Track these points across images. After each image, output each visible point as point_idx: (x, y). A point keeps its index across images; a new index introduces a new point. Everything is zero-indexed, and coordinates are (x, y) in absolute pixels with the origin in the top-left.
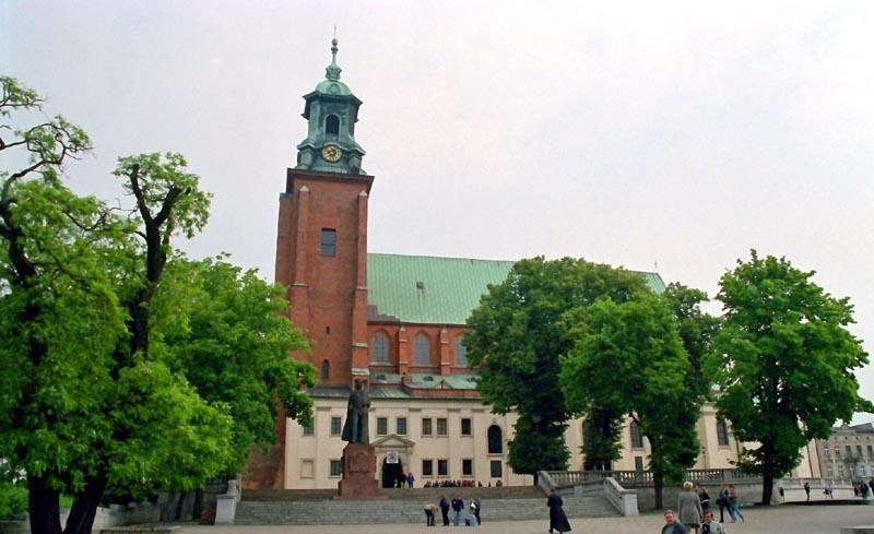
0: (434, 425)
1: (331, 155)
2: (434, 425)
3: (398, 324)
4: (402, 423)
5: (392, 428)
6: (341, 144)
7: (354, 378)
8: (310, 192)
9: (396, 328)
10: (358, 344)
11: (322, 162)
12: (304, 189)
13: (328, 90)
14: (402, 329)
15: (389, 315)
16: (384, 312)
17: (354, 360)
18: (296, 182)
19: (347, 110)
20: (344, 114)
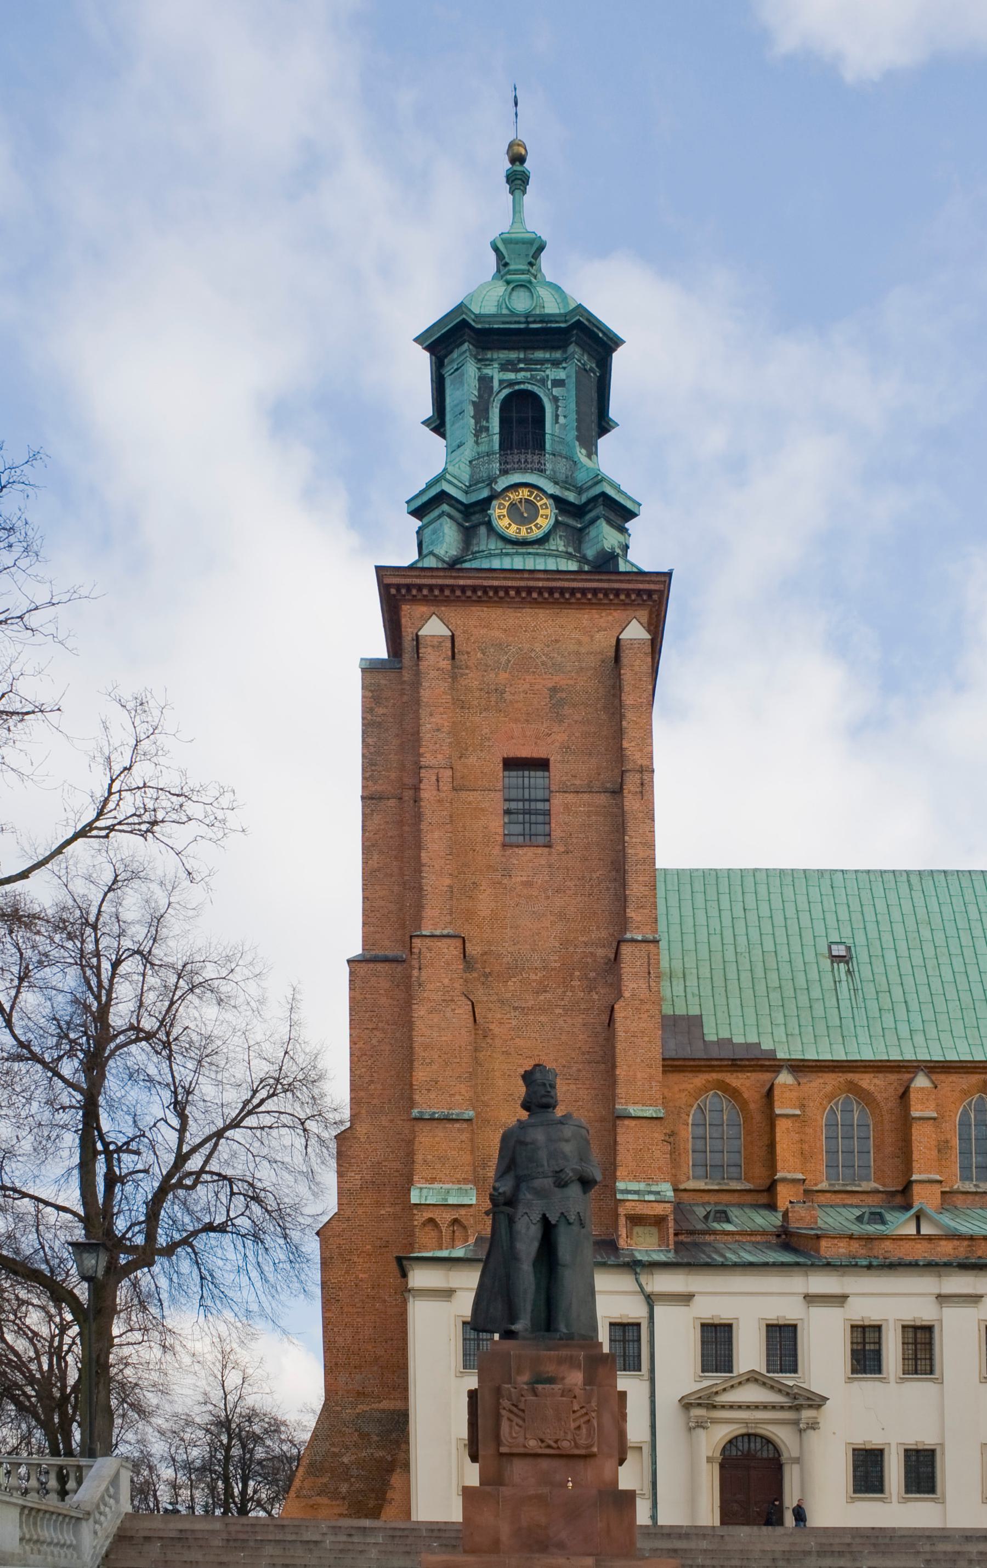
3: (769, 1064)
7: (622, 1211)
8: (453, 637)
9: (767, 1076)
10: (633, 1110)
11: (494, 545)
13: (499, 306)
14: (785, 1078)
16: (725, 1034)
17: (624, 1156)
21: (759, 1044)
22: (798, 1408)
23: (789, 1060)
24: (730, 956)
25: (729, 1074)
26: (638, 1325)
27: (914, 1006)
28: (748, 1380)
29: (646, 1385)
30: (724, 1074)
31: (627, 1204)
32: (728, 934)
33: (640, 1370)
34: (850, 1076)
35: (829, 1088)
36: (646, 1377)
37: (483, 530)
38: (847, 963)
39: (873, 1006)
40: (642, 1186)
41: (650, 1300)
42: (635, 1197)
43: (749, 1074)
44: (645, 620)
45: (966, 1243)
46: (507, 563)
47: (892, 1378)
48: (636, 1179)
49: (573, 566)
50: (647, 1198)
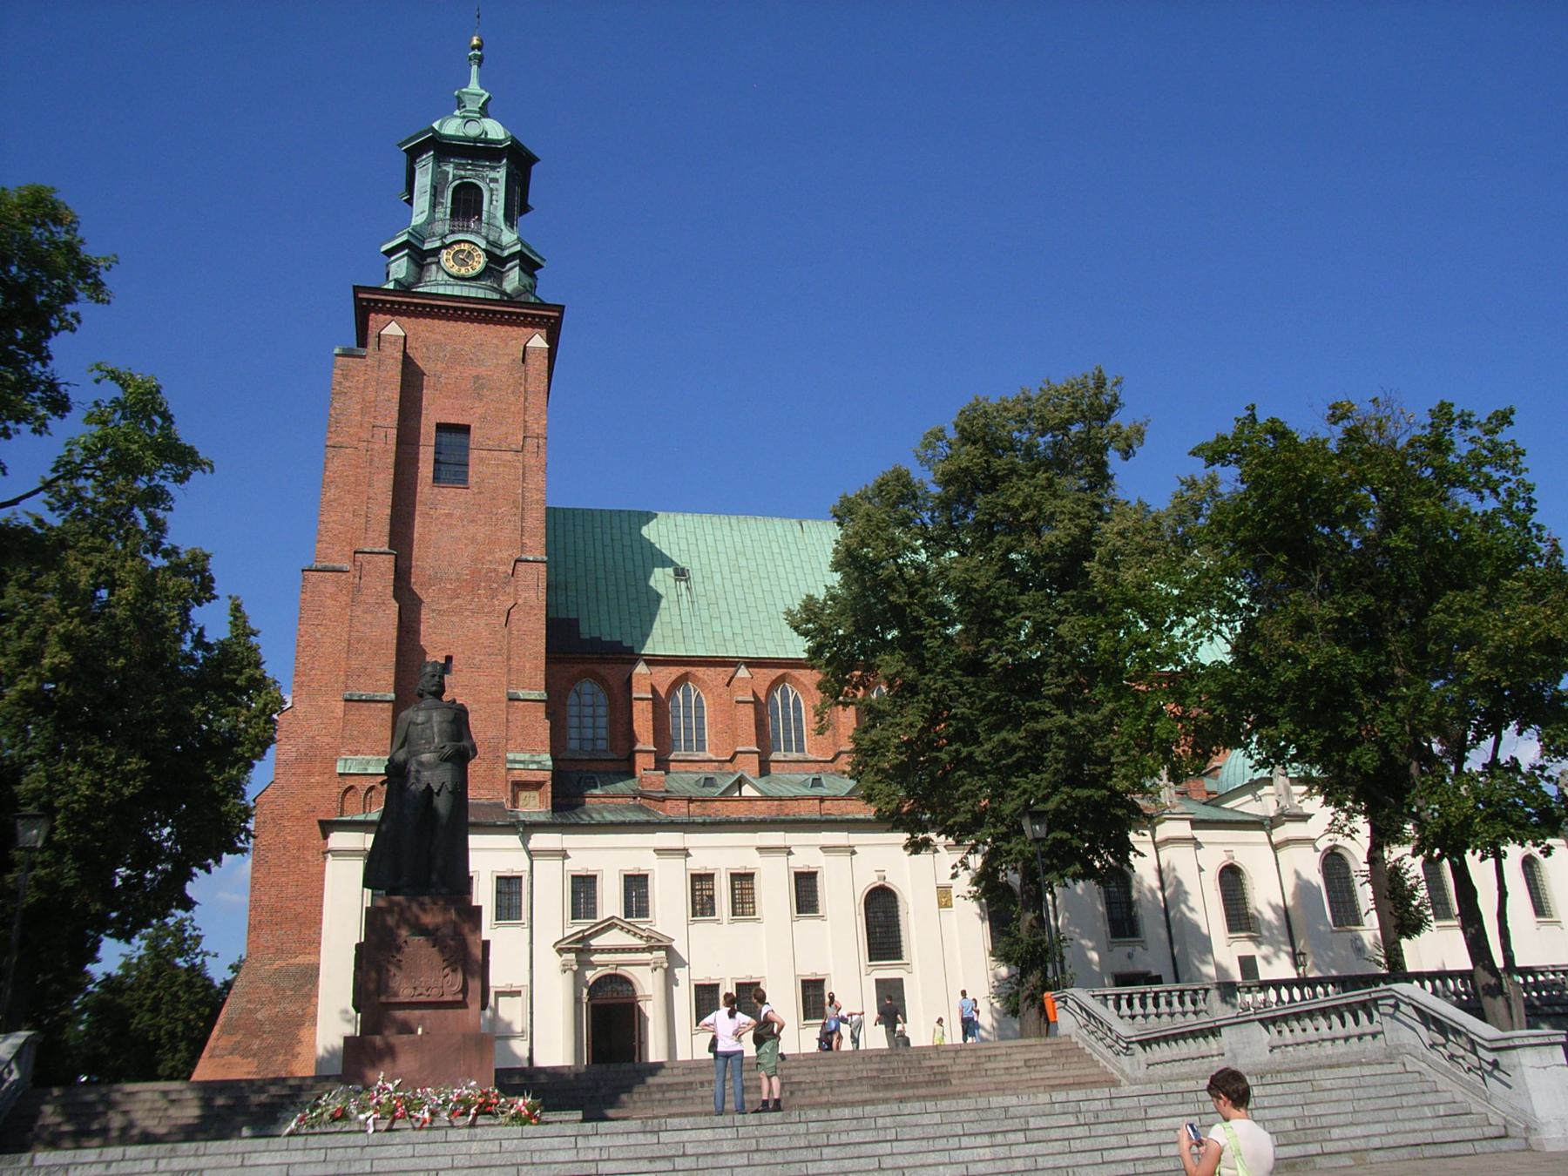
0: (723, 892)
1: (464, 263)
2: (723, 892)
4: (636, 886)
5: (610, 901)
6: (486, 238)
11: (442, 277)
12: (393, 329)
15: (606, 638)
16: (596, 634)
18: (375, 320)
19: (501, 174)
20: (495, 180)
21: (621, 642)
22: (650, 949)
24: (601, 574)
26: (520, 878)
27: (735, 615)
29: (528, 930)
32: (600, 556)
33: (520, 918)
34: (688, 669)
35: (673, 677)
37: (434, 267)
38: (686, 581)
39: (705, 614)
41: (531, 854)
42: (521, 766)
44: (545, 335)
46: (449, 291)
47: (725, 921)
48: (522, 751)
49: (496, 296)
50: (531, 767)
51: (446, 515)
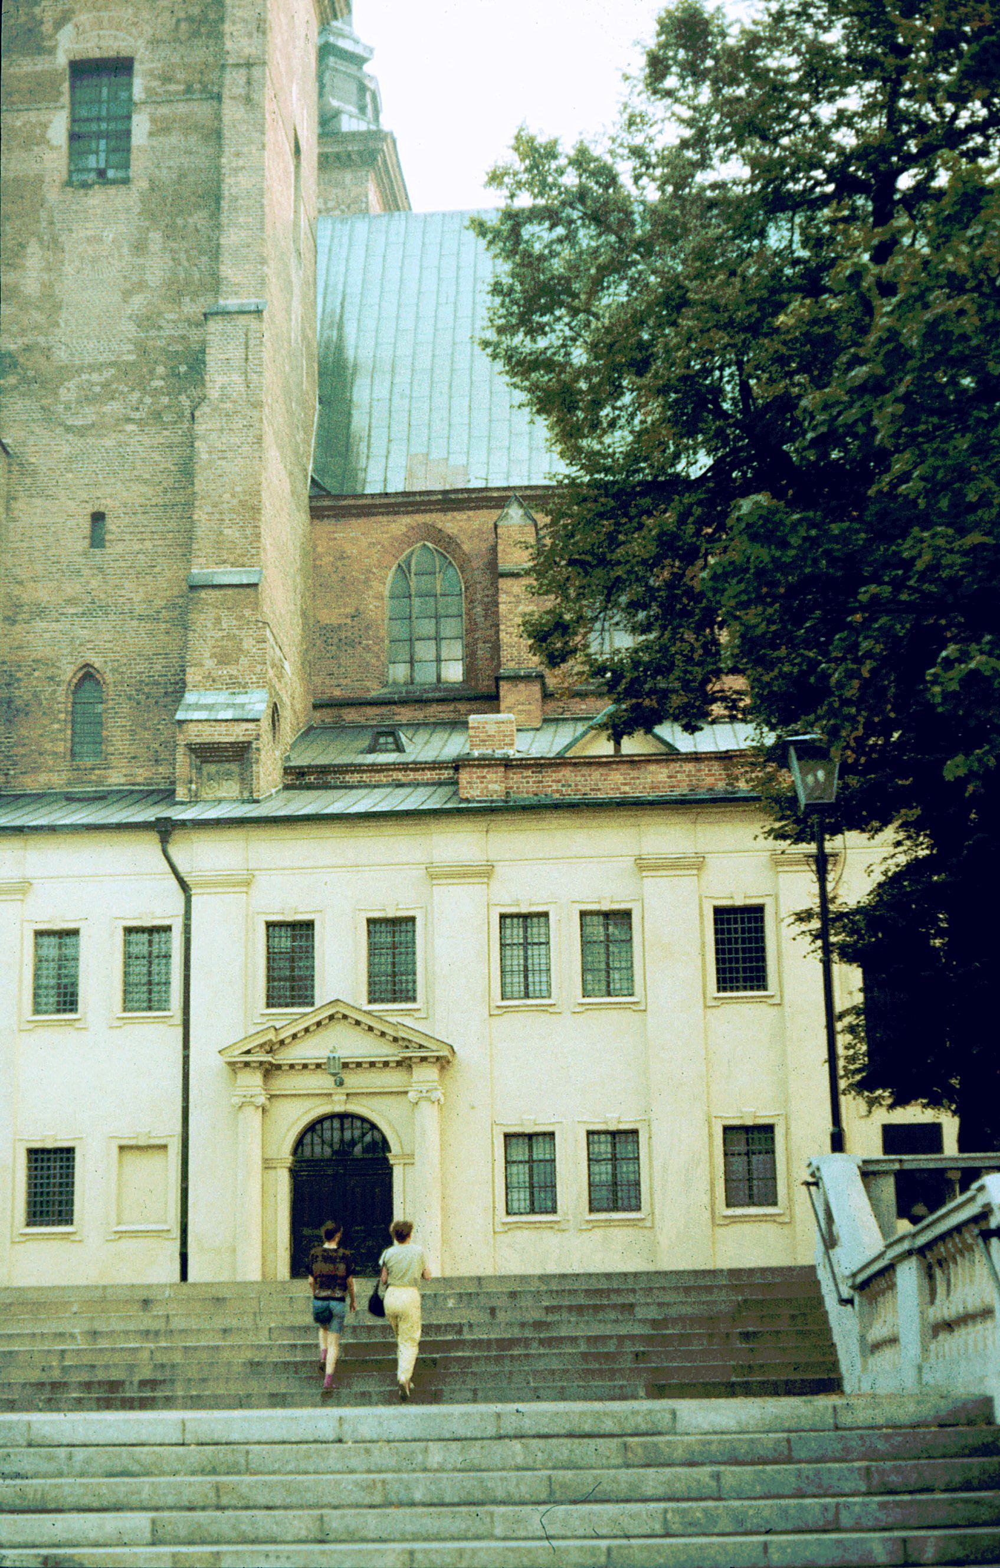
7: (181, 740)
22: (405, 1064)
23: (527, 488)
25: (440, 515)
28: (331, 1017)
30: (434, 515)
31: (191, 725)
36: (178, 1018)
40: (222, 697)
43: (471, 513)
45: (689, 767)
51: (88, 240)
